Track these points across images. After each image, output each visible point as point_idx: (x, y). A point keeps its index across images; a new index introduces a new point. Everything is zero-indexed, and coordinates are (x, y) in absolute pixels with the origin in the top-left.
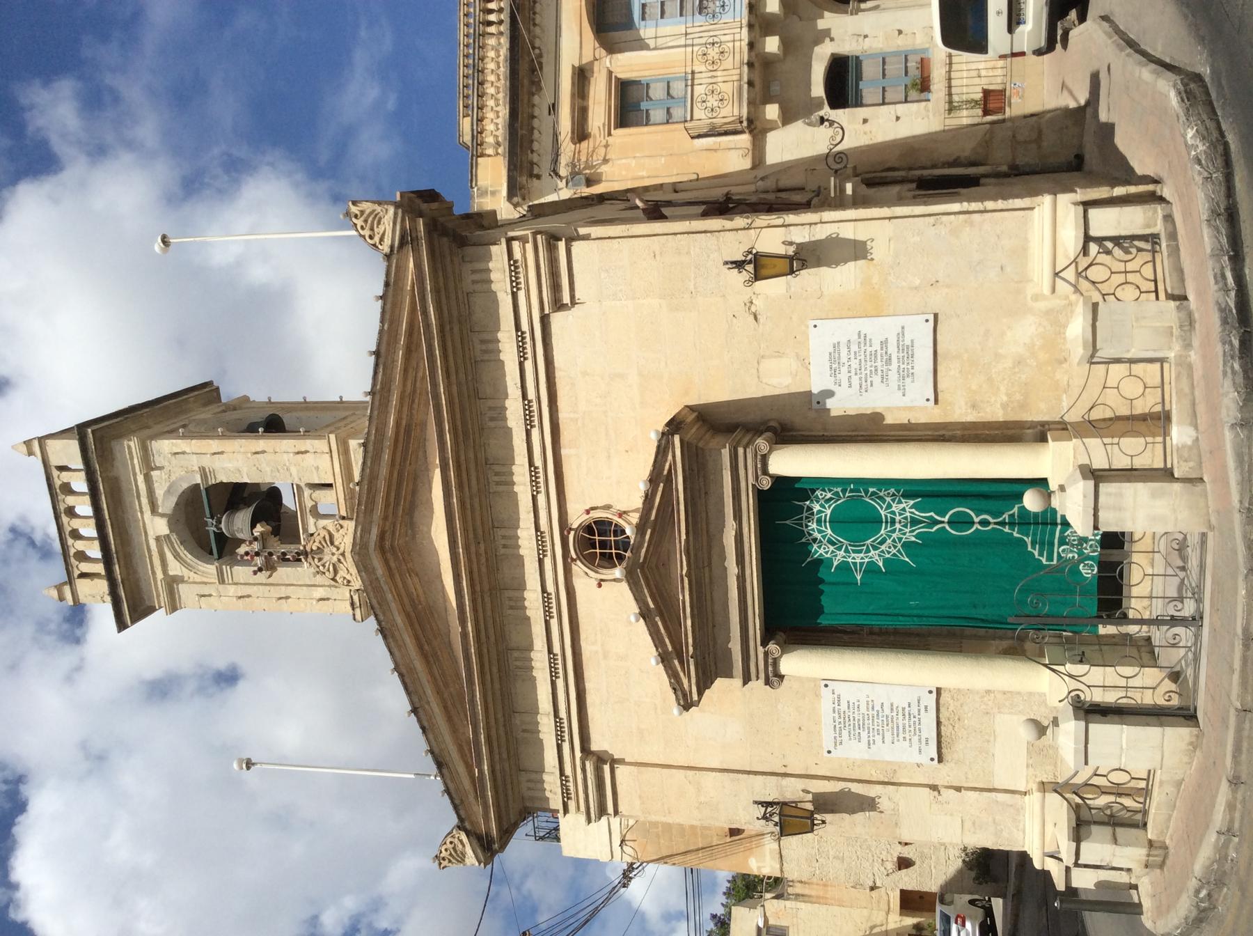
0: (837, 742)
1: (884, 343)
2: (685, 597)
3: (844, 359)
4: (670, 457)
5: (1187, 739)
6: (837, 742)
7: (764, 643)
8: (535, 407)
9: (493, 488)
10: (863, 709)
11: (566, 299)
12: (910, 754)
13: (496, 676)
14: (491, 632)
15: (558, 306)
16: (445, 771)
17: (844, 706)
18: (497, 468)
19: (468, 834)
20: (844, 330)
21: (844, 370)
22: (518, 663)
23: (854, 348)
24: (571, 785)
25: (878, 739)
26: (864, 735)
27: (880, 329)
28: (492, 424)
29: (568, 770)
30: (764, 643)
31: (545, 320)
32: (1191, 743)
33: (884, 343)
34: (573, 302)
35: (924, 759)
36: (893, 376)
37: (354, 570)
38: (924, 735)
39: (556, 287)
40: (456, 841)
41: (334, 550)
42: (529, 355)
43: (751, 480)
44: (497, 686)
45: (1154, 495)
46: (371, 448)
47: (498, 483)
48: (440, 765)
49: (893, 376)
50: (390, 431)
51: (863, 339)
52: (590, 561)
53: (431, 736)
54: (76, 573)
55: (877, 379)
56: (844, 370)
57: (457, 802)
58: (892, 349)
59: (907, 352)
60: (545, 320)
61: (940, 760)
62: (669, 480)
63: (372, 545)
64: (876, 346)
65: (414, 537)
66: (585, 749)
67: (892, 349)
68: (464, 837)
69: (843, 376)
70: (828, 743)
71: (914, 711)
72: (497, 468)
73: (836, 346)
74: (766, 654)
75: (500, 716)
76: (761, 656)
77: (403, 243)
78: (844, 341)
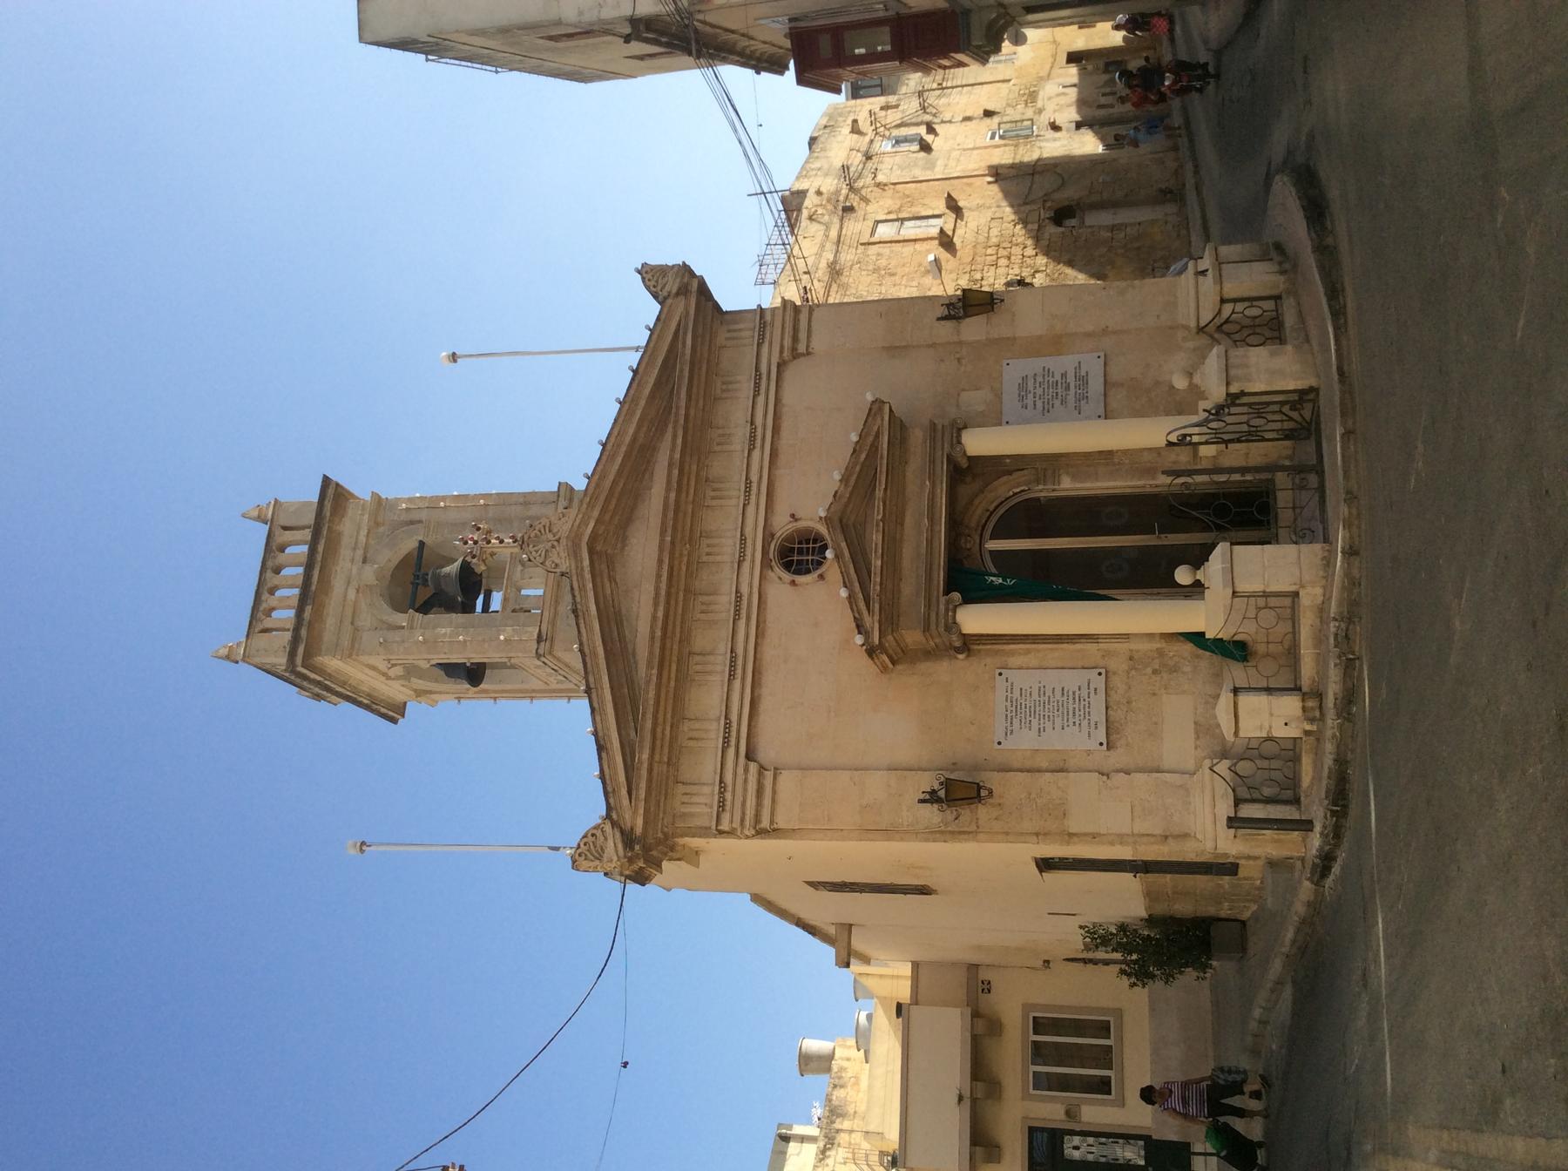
0: (1008, 732)
1: (1064, 375)
2: (876, 538)
3: (1031, 387)
4: (879, 421)
5: (1320, 554)
6: (1008, 732)
7: (947, 592)
8: (759, 431)
9: (709, 502)
10: (1035, 696)
11: (802, 348)
12: (1081, 740)
13: (673, 675)
14: (678, 630)
15: (796, 355)
16: (604, 755)
17: (1017, 693)
18: (716, 485)
19: (614, 824)
20: (1034, 365)
21: (1031, 396)
22: (698, 668)
23: (1040, 379)
24: (728, 796)
25: (1049, 725)
26: (1035, 723)
27: (1064, 364)
28: (718, 448)
29: (729, 778)
30: (947, 592)
31: (781, 366)
32: (1324, 558)
33: (1064, 375)
34: (808, 353)
35: (1093, 745)
36: (1071, 398)
37: (563, 555)
38: (1094, 718)
39: (795, 339)
40: (599, 833)
41: (550, 536)
42: (763, 391)
43: (947, 449)
44: (672, 683)
45: (1272, 354)
46: (609, 447)
47: (713, 498)
48: (601, 748)
49: (1071, 398)
50: (628, 439)
51: (1047, 372)
52: (788, 566)
53: (598, 718)
54: (260, 627)
55: (1057, 403)
56: (1031, 396)
57: (609, 789)
58: (1071, 379)
59: (1083, 381)
60: (781, 366)
61: (1109, 748)
62: (874, 447)
63: (586, 538)
64: (1058, 377)
65: (623, 548)
66: (750, 757)
67: (1071, 379)
68: (608, 827)
69: (1029, 400)
70: (1000, 736)
71: (1084, 693)
72: (716, 485)
73: (1025, 379)
74: (948, 603)
75: (669, 716)
76: (942, 607)
77: (677, 294)
78: (1031, 374)
